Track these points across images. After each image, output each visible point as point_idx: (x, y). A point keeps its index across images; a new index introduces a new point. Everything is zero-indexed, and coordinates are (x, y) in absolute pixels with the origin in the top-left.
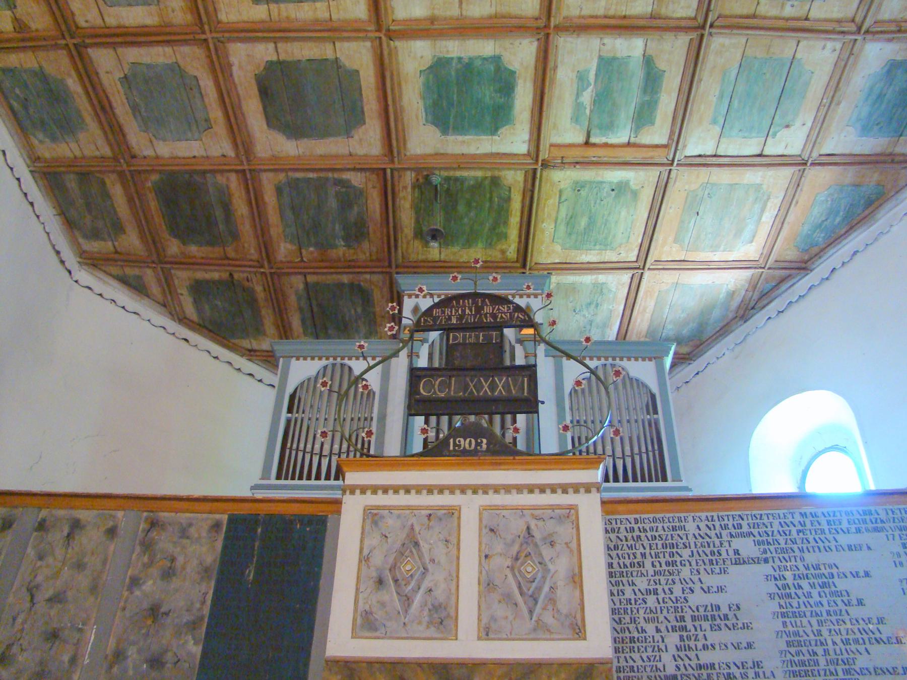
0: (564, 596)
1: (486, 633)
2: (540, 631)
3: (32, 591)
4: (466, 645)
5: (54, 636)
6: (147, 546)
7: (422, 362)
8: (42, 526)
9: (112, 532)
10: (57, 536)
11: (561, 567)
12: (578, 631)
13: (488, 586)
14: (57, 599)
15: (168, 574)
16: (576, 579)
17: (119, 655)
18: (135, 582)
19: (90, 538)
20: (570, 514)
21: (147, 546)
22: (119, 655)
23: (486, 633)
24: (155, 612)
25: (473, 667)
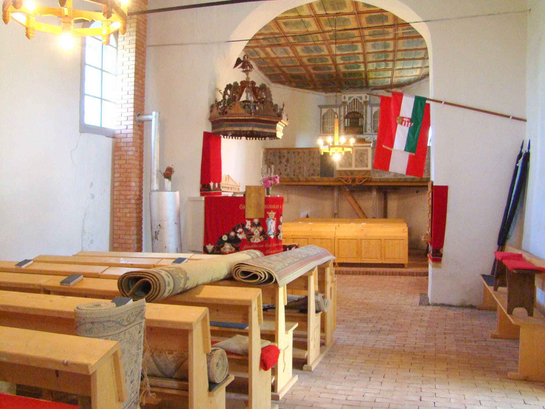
0: (366, 161)
1: (356, 166)
2: (362, 166)
3: (295, 162)
4: (353, 168)
5: (300, 168)
6: (310, 155)
7: (346, 125)
8: (294, 153)
9: (304, 153)
10: (297, 154)
11: (365, 157)
12: (367, 166)
13: (356, 160)
14: (299, 163)
15: (313, 159)
16: (367, 159)
17: (309, 170)
18: (309, 160)
19: (301, 154)
20: (367, 150)
21: (310, 155)
22: (309, 170)
23: (356, 166)
24: (313, 164)
25: (354, 171)
